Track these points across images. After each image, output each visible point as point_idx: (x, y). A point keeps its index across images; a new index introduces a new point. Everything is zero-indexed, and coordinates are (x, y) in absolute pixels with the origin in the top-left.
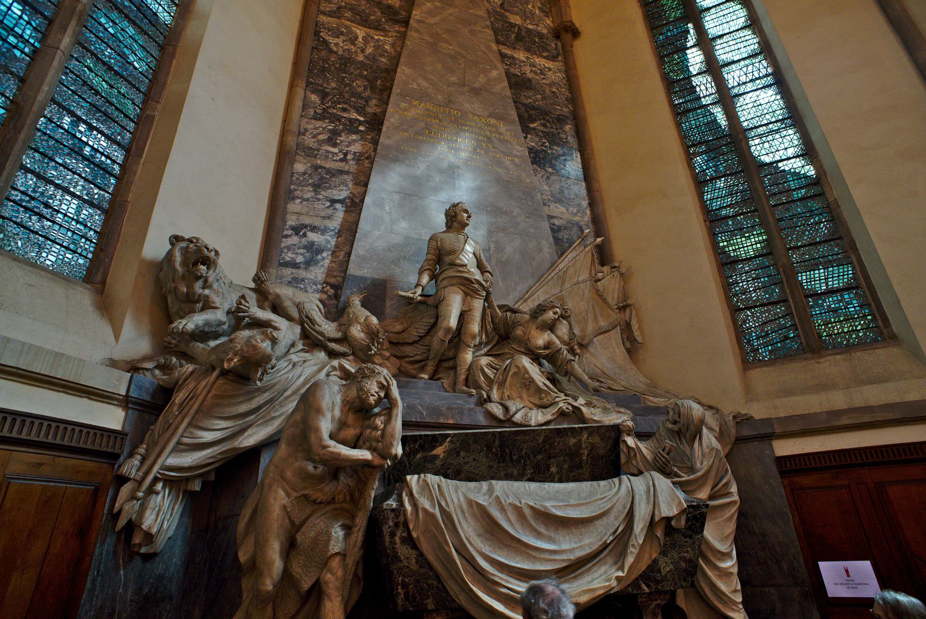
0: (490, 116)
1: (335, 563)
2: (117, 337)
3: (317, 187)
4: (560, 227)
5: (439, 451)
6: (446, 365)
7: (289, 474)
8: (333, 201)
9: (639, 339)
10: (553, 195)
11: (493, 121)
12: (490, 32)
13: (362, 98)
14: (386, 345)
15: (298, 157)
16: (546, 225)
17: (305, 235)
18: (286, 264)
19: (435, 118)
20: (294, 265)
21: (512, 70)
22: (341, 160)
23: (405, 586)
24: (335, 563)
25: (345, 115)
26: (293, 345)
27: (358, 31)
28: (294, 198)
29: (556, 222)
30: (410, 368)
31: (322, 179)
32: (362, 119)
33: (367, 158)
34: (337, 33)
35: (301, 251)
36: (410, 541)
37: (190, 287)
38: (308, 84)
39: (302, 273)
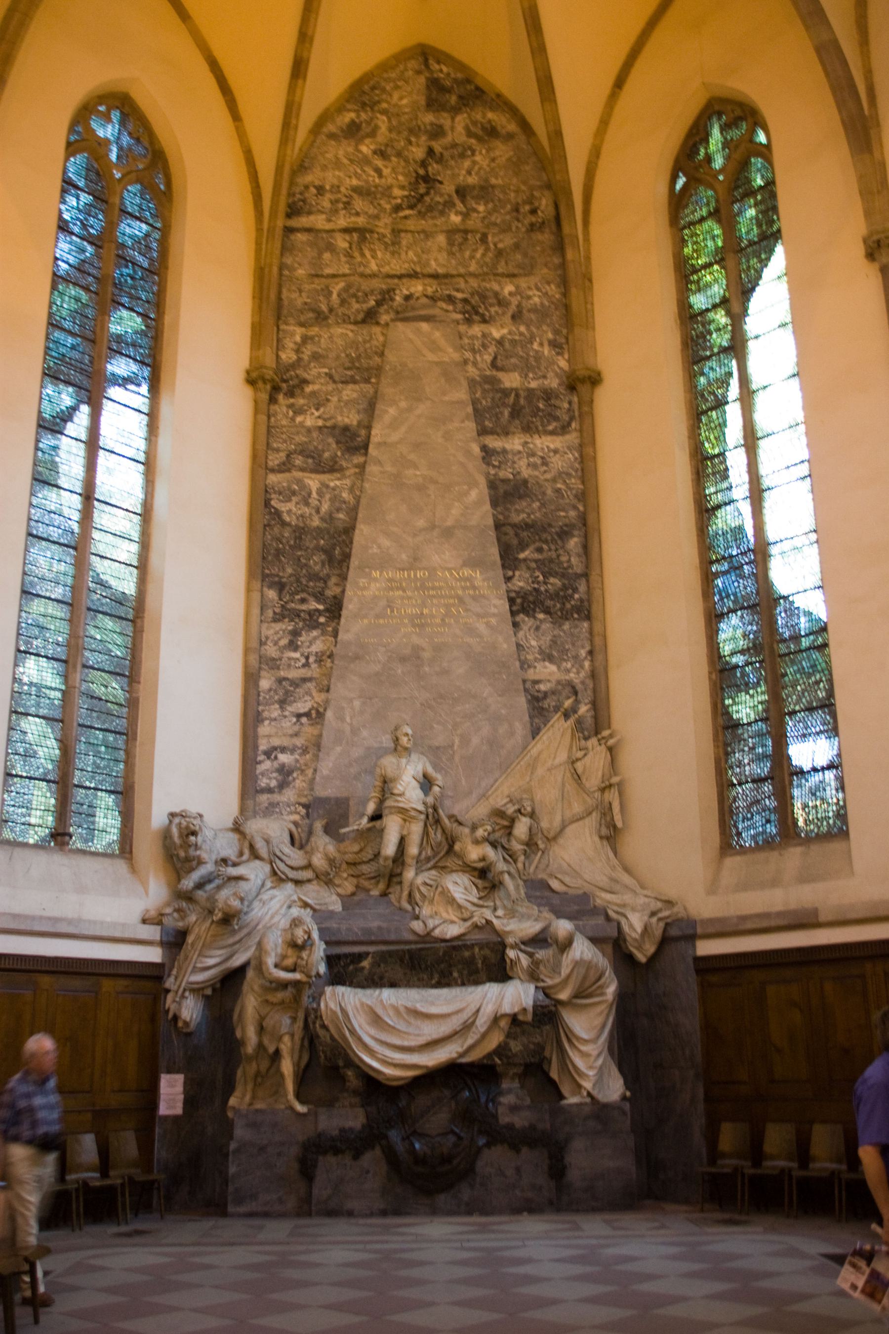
0: (465, 564)
1: (286, 1039)
2: (147, 893)
3: (282, 703)
4: (546, 695)
5: (366, 964)
6: (395, 880)
7: (256, 988)
8: (299, 716)
9: (619, 824)
10: (541, 651)
11: (467, 572)
12: (471, 425)
13: (321, 579)
14: (344, 866)
15: (263, 673)
16: (522, 702)
17: (276, 758)
18: (263, 791)
19: (398, 589)
20: (270, 790)
21: (502, 474)
22: (304, 666)
23: (323, 1052)
24: (286, 1039)
25: (304, 607)
26: (263, 885)
27: (311, 483)
28: (262, 721)
29: (542, 687)
30: (366, 884)
31: (287, 692)
32: (321, 607)
33: (329, 657)
34: (288, 494)
35: (275, 775)
36: (324, 1027)
37: (186, 852)
38: (264, 577)
39: (276, 797)
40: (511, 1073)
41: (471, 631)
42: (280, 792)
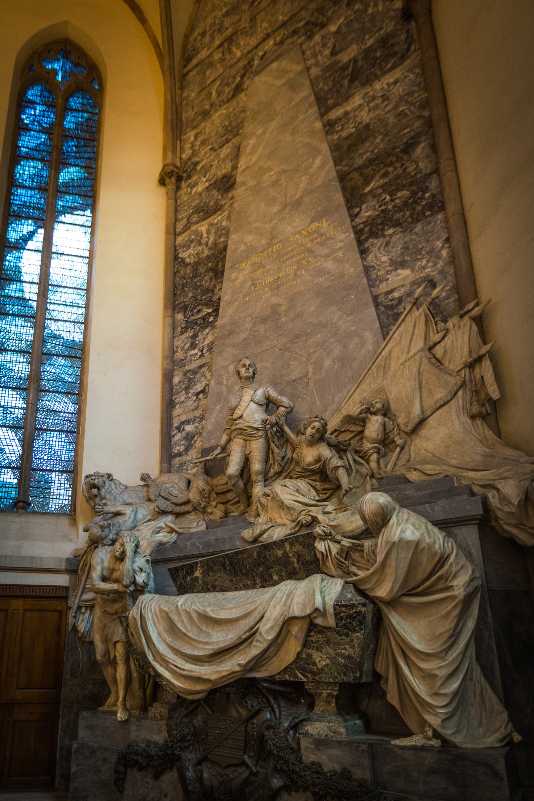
39: (185, 458)
40: (325, 693)
41: (320, 272)
42: (186, 454)
